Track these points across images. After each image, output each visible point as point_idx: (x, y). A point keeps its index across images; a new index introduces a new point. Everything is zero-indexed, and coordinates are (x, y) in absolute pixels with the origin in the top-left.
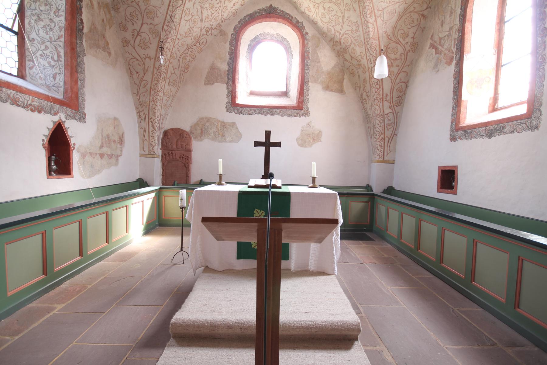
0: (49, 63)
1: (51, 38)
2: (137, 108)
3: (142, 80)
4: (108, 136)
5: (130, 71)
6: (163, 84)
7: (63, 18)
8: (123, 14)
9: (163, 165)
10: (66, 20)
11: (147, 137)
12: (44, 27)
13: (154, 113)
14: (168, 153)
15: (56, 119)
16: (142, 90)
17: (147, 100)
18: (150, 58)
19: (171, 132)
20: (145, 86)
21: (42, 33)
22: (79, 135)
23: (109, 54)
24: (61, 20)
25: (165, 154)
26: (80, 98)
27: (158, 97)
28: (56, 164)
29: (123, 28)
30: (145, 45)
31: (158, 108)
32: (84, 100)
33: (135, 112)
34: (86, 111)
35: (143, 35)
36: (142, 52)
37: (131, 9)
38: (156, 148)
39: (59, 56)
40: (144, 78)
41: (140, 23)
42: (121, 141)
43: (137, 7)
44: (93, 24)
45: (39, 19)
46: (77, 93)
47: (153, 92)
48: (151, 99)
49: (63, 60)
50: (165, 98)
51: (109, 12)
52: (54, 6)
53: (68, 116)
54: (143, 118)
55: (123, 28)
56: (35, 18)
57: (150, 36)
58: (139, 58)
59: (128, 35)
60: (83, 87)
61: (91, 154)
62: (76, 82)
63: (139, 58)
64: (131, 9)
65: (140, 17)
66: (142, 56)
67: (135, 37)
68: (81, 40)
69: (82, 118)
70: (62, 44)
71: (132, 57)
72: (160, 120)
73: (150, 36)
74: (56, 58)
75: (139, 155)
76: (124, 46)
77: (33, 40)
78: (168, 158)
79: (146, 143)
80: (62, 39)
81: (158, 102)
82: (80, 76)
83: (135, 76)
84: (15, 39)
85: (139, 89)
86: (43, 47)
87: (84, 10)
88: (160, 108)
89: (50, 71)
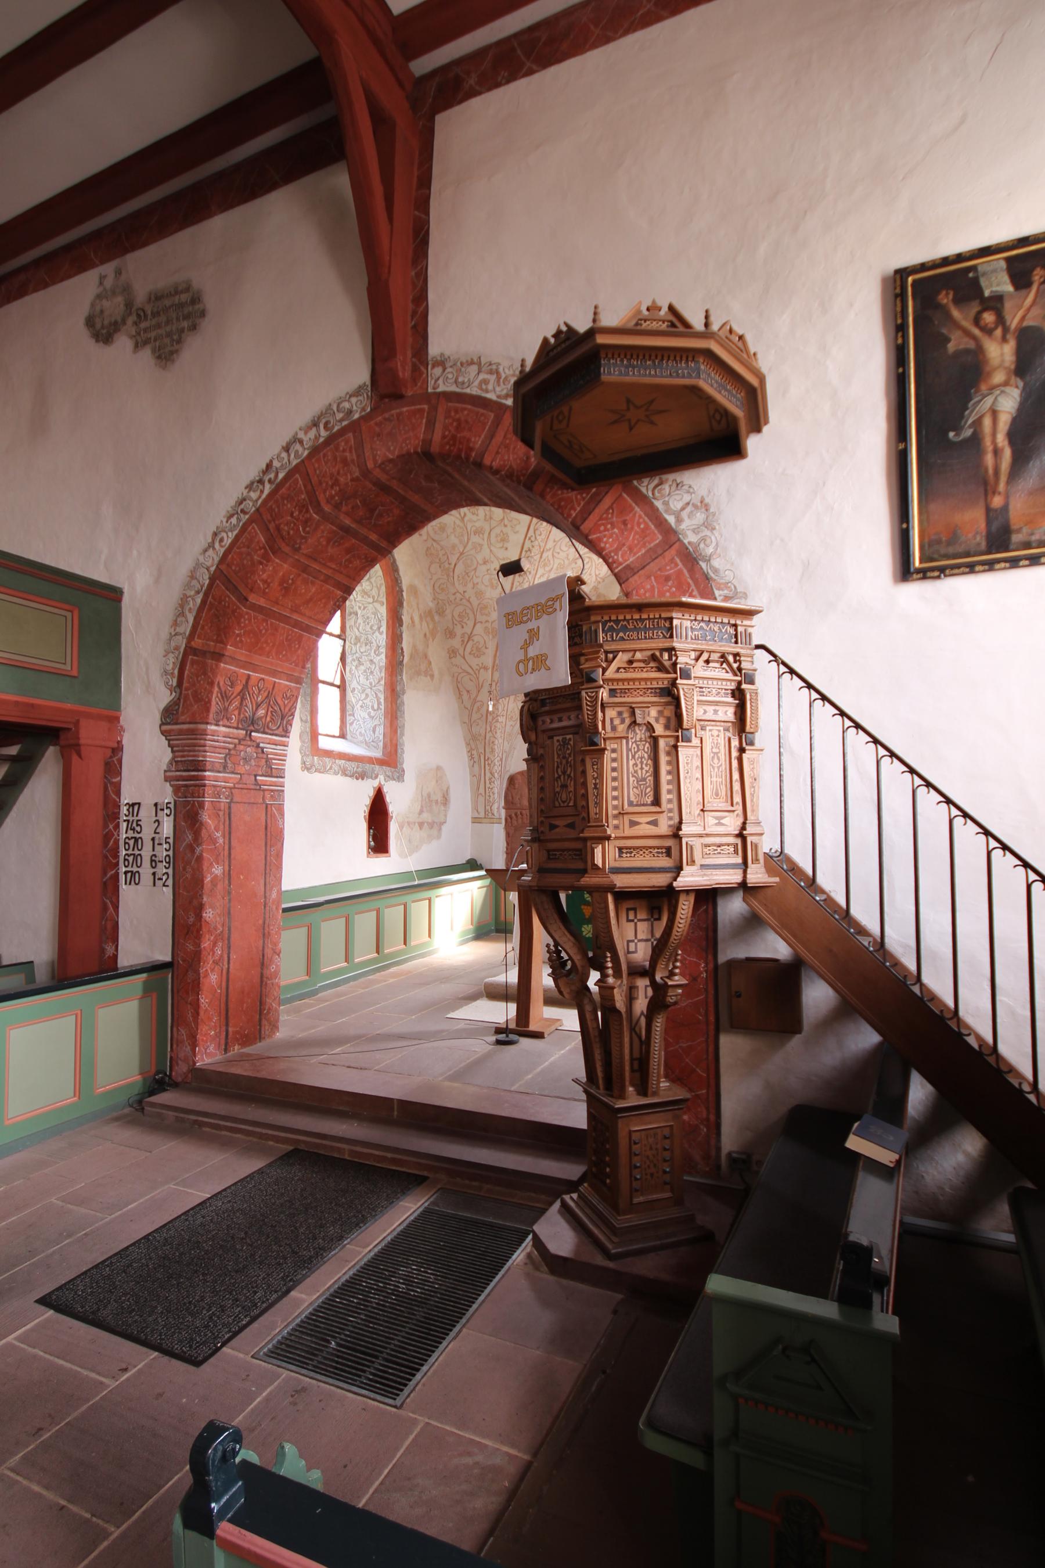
0: (369, 714)
1: (371, 684)
2: (468, 744)
3: (475, 701)
4: (429, 796)
5: (459, 692)
6: (506, 702)
7: (383, 656)
8: (450, 617)
9: (508, 835)
10: (386, 657)
11: (482, 790)
12: (365, 671)
13: (493, 750)
14: (516, 815)
15: (375, 783)
16: (475, 716)
17: (482, 731)
18: (486, 668)
19: (519, 777)
20: (479, 709)
21: (362, 679)
22: (400, 801)
23: (432, 676)
24: (381, 659)
25: (511, 818)
26: (399, 751)
27: (498, 725)
28: (374, 840)
29: (450, 634)
30: (478, 652)
31: (499, 741)
32: (403, 752)
33: (465, 750)
34: (405, 766)
35: (476, 639)
36: (474, 662)
37: (460, 609)
38: (495, 806)
39: (379, 704)
40: (479, 698)
41: (471, 623)
42: (446, 801)
43: (468, 604)
44: (414, 647)
45: (360, 663)
46: (396, 745)
47: (490, 718)
48: (488, 729)
49: (382, 707)
50: (509, 723)
51: (433, 619)
52: (374, 644)
53: (388, 778)
54: (476, 759)
55: (450, 634)
56: (355, 664)
57: (486, 638)
58: (470, 671)
59: (456, 643)
60: (403, 734)
61: (409, 823)
62: (396, 732)
63: (470, 671)
64: (460, 609)
65: (471, 616)
66: (475, 667)
67: (464, 644)
68: (401, 675)
69: (400, 778)
70: (382, 688)
71: (460, 671)
72: (501, 760)
73: (486, 638)
74: (376, 707)
75: (470, 820)
76: (450, 658)
77: (354, 689)
78: (515, 823)
79: (481, 799)
80: (383, 682)
81: (498, 732)
82: (399, 722)
83: (465, 696)
84: (336, 692)
85: (470, 716)
86: (363, 696)
87: (404, 636)
88: (501, 741)
89: (370, 724)
